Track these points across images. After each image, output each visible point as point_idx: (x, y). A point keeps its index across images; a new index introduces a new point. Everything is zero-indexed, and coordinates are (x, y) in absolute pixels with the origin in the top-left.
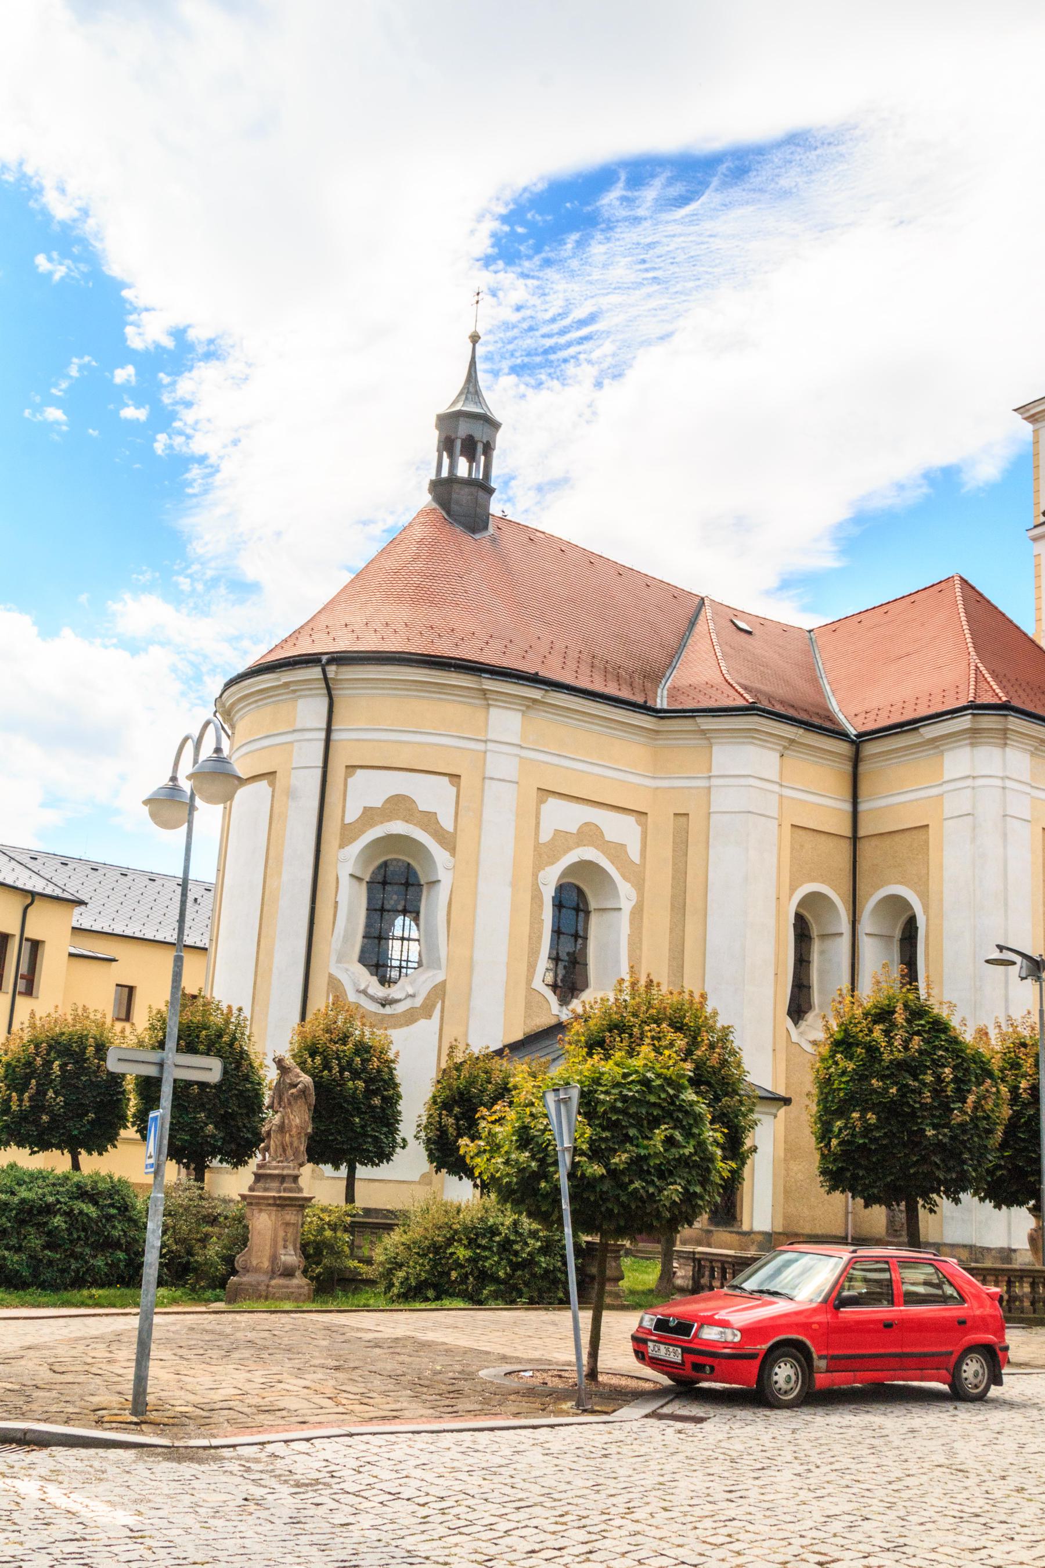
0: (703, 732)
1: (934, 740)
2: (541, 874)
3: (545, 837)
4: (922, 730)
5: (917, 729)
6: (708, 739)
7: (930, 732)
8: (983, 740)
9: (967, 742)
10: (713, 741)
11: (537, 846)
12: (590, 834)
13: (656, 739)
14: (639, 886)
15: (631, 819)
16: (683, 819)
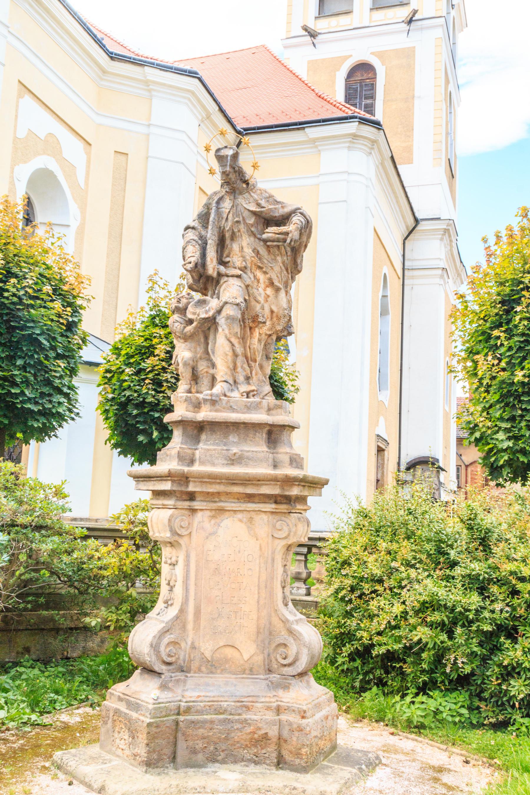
0: (147, 83)
1: (314, 141)
2: (16, 168)
3: (22, 134)
4: (306, 130)
5: (303, 128)
6: (150, 91)
7: (312, 132)
8: (356, 146)
9: (347, 145)
10: (154, 93)
11: (15, 138)
12: (51, 145)
13: (102, 79)
14: (83, 209)
15: (80, 144)
16: (123, 158)
